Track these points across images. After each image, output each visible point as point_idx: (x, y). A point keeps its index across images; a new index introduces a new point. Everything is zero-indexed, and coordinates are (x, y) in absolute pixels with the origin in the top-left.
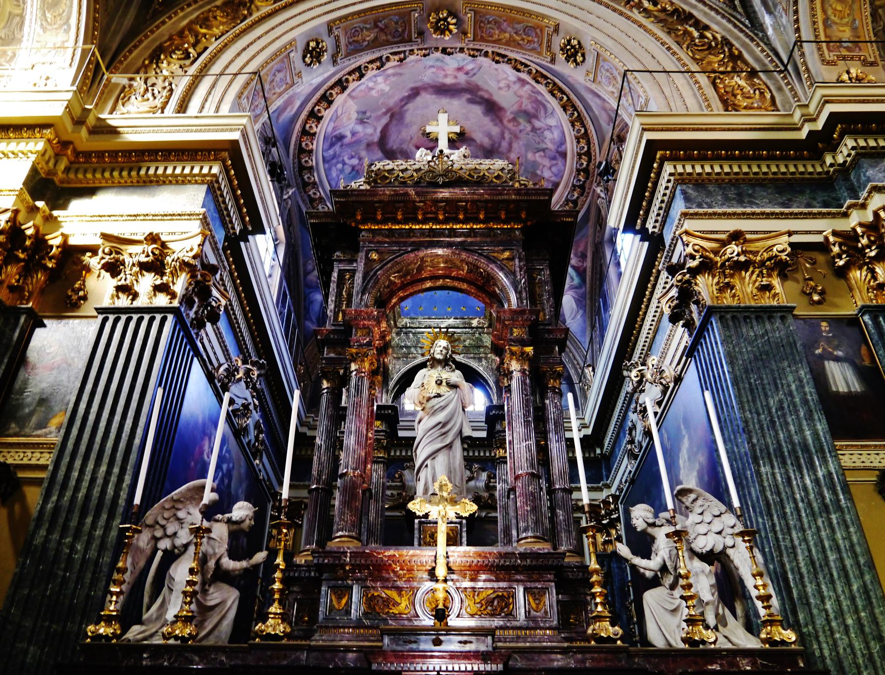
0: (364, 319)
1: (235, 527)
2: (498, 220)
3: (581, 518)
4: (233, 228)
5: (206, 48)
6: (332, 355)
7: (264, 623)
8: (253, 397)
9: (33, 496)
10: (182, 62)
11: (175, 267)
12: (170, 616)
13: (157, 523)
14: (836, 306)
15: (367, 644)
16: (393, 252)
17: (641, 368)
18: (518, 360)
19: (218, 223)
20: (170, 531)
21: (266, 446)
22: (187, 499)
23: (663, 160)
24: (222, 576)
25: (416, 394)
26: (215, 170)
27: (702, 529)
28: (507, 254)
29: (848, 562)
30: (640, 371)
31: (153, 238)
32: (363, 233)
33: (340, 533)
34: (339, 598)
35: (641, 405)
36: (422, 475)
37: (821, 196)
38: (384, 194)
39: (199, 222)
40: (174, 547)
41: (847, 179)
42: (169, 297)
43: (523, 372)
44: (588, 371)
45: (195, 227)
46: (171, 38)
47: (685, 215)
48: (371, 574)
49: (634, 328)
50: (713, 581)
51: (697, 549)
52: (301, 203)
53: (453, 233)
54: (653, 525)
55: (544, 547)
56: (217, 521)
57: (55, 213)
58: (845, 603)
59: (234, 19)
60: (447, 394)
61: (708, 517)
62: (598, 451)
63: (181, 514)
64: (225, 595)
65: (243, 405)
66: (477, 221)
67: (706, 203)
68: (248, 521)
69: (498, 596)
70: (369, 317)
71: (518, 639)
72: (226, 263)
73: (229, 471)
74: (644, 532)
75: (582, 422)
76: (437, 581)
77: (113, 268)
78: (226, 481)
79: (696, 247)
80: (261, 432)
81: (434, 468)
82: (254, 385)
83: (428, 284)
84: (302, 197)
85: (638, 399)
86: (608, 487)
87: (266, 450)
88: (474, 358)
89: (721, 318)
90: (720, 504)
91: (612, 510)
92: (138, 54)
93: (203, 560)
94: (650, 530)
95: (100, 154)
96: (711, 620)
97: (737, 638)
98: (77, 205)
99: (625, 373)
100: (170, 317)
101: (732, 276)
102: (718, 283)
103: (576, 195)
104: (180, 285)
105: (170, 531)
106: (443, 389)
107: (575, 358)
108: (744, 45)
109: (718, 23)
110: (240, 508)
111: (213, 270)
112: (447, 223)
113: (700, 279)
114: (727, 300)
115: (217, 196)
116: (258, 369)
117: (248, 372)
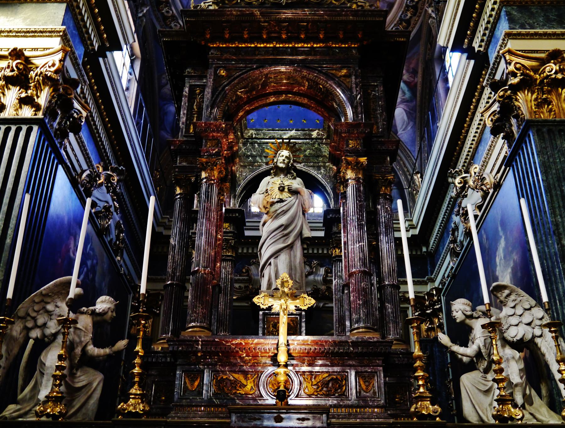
0: (214, 131)
1: (99, 318)
2: (336, 40)
3: (408, 308)
4: (92, 44)
6: (184, 164)
7: (126, 402)
8: (113, 200)
11: (38, 81)
12: (43, 394)
13: (28, 315)
15: (216, 420)
16: (240, 69)
17: (464, 175)
18: (353, 169)
19: (77, 40)
20: (40, 321)
21: (126, 244)
22: (55, 294)
25: (261, 200)
27: (514, 320)
28: (344, 72)
30: (463, 178)
32: (212, 51)
33: (193, 324)
34: (192, 381)
35: (463, 209)
36: (266, 272)
38: (232, 14)
39: (59, 39)
40: (44, 335)
42: (34, 109)
43: (357, 180)
44: (417, 177)
45: (55, 43)
47: (509, 36)
48: (220, 360)
49: (459, 139)
50: (522, 366)
51: (509, 338)
52: (155, 20)
53: (295, 51)
54: (471, 317)
55: (374, 337)
56: (83, 313)
60: (289, 199)
61: (519, 311)
62: (424, 249)
63: (50, 307)
64: (91, 378)
65: (105, 207)
66: (318, 41)
67: (529, 24)
68: (110, 313)
69: (332, 379)
70: (218, 129)
71: (349, 416)
72: (86, 78)
73: (93, 266)
74: (463, 322)
75: (410, 223)
76: (279, 366)
78: (91, 276)
79: (518, 66)
80: (121, 231)
81: (276, 266)
82: (115, 189)
83: (272, 99)
84: (156, 16)
85: (461, 203)
87: (126, 248)
88: (313, 166)
89: (538, 131)
90: (531, 299)
91: (436, 302)
93: (70, 347)
94: (468, 321)
96: (519, 399)
97: (542, 415)
99: (450, 180)
100: (35, 128)
101: (549, 92)
102: (536, 99)
103: (409, 15)
104: (43, 99)
105: (40, 321)
107: (405, 166)
110: (102, 302)
111: (74, 84)
112: (289, 43)
113: (520, 95)
114: (544, 115)
115: (75, 14)
116: (117, 176)
117: (108, 177)
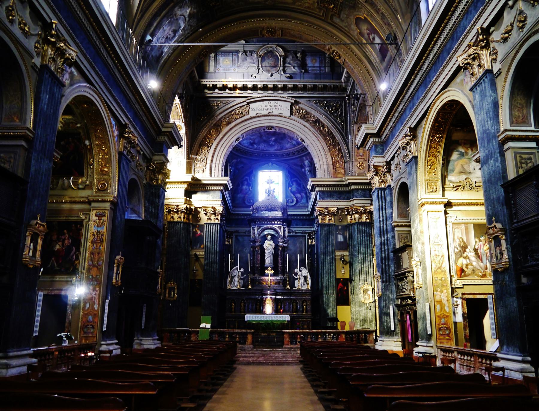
5: (212, 144)
9: (202, 260)
10: (207, 149)
14: (344, 222)
23: (316, 187)
24: (241, 279)
26: (222, 188)
29: (332, 272)
31: (212, 207)
37: (348, 195)
41: (353, 192)
45: (220, 203)
46: (202, 141)
57: (190, 199)
58: (329, 278)
59: (218, 131)
77: (206, 214)
86: (314, 227)
92: (196, 147)
93: (238, 277)
95: (197, 184)
98: (193, 196)
100: (219, 225)
106: (270, 246)
108: (342, 146)
109: (337, 137)
